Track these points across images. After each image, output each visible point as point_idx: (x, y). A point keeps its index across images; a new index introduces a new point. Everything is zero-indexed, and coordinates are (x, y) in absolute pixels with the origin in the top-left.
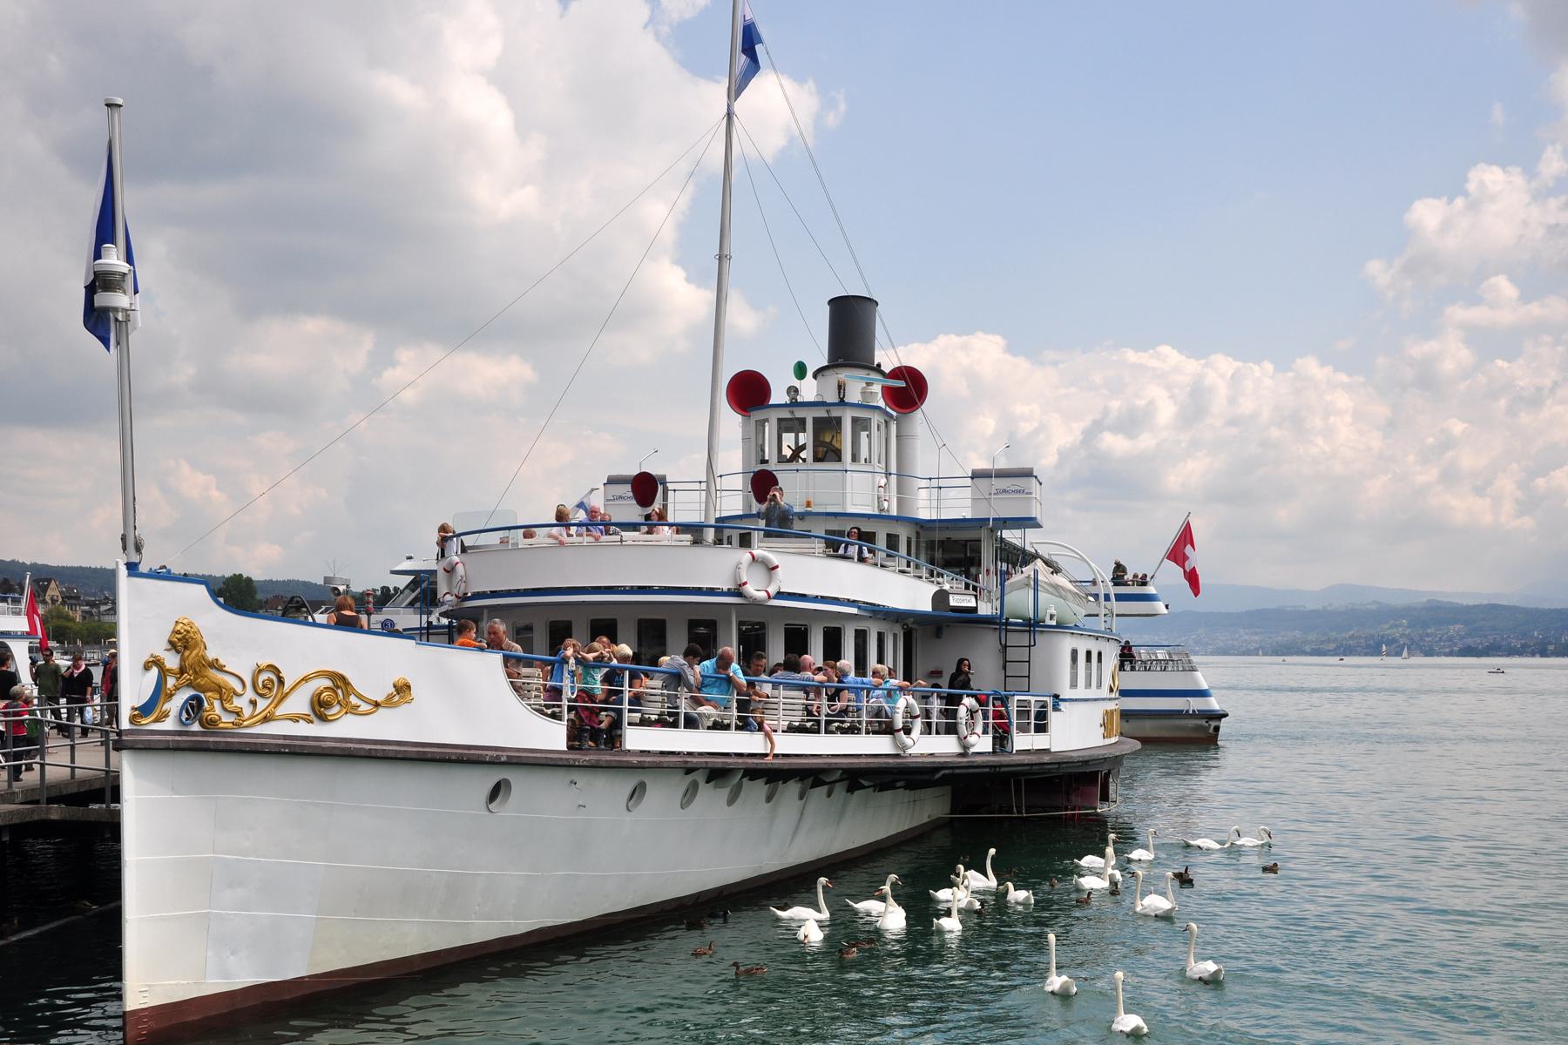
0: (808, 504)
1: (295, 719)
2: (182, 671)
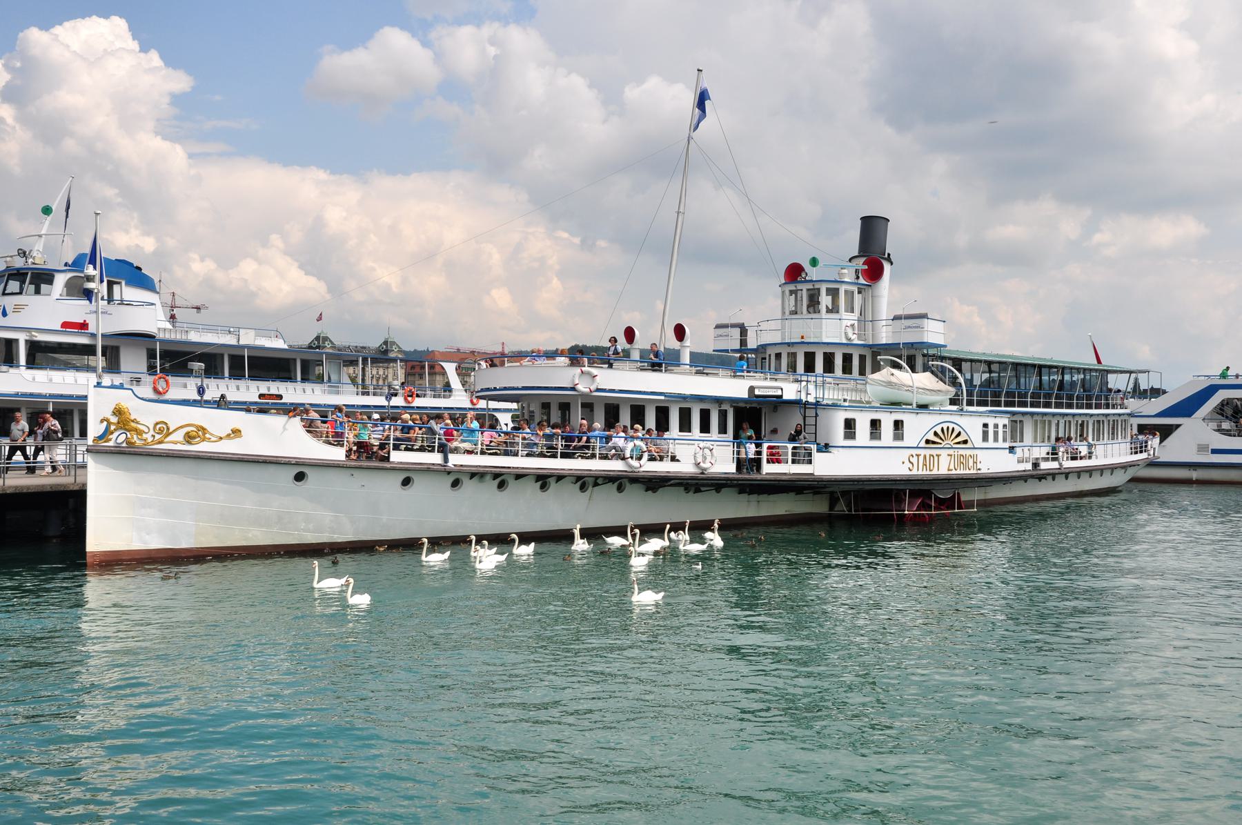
0: (802, 337)
2: (118, 423)
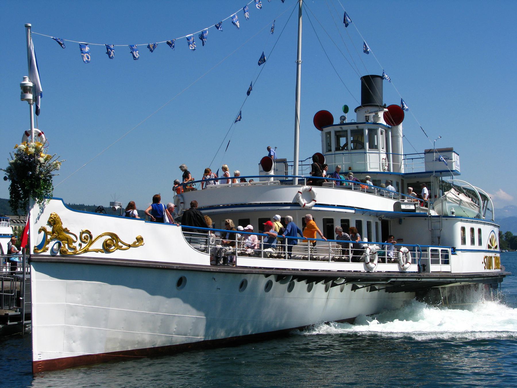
1: (97, 251)
2: (53, 232)
